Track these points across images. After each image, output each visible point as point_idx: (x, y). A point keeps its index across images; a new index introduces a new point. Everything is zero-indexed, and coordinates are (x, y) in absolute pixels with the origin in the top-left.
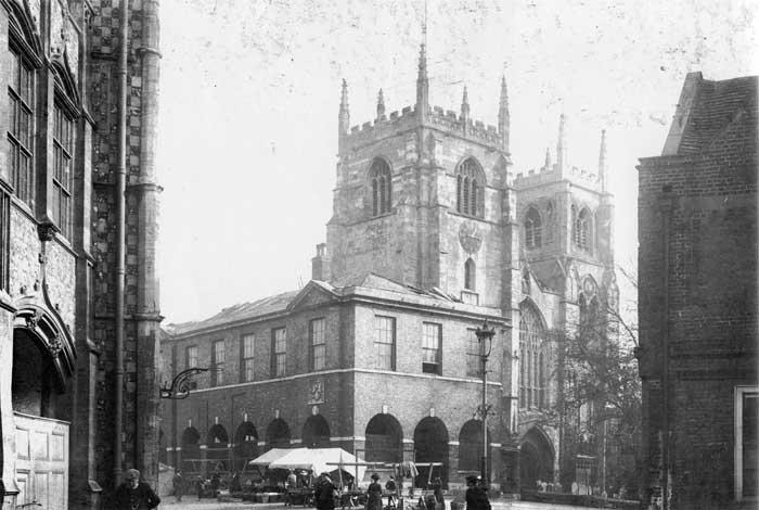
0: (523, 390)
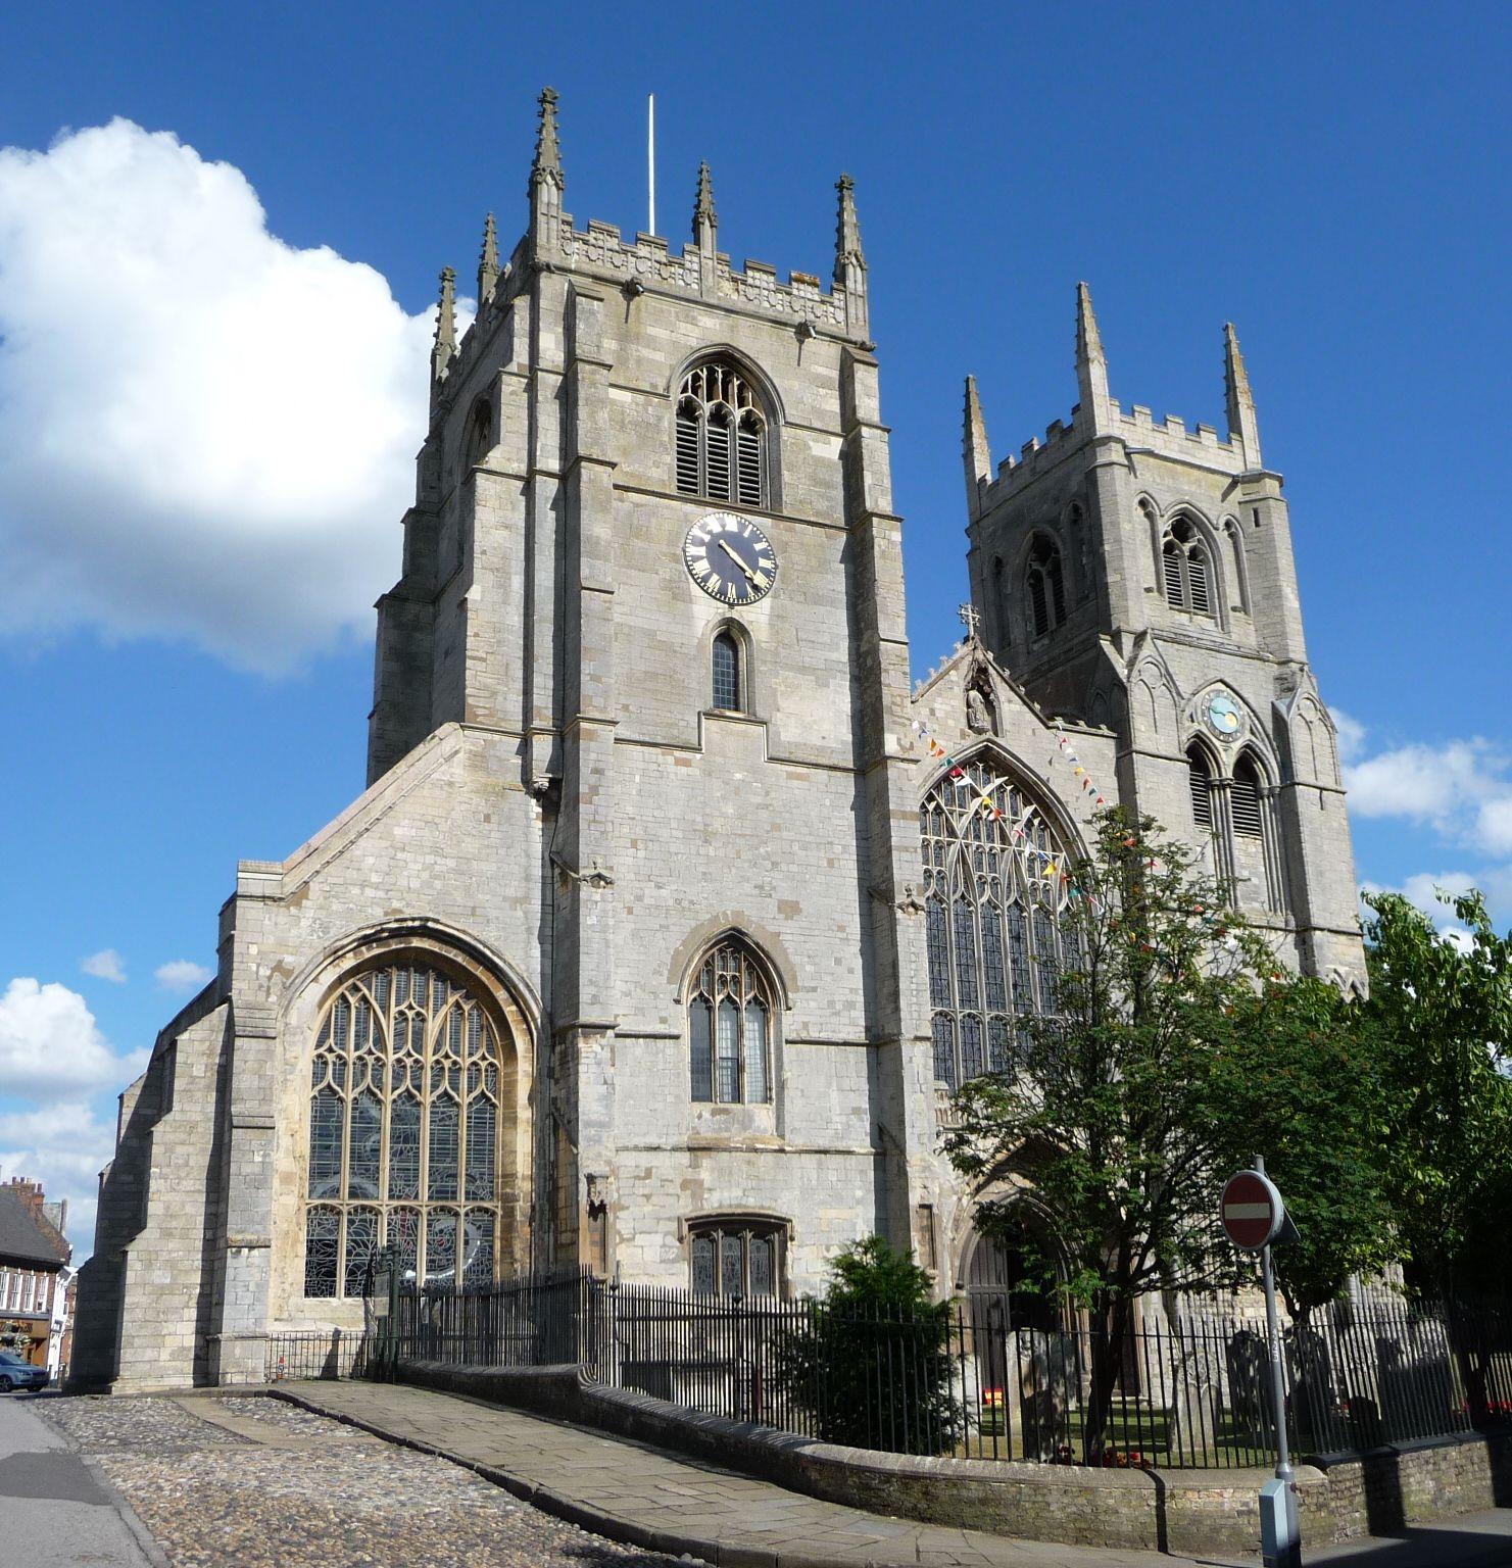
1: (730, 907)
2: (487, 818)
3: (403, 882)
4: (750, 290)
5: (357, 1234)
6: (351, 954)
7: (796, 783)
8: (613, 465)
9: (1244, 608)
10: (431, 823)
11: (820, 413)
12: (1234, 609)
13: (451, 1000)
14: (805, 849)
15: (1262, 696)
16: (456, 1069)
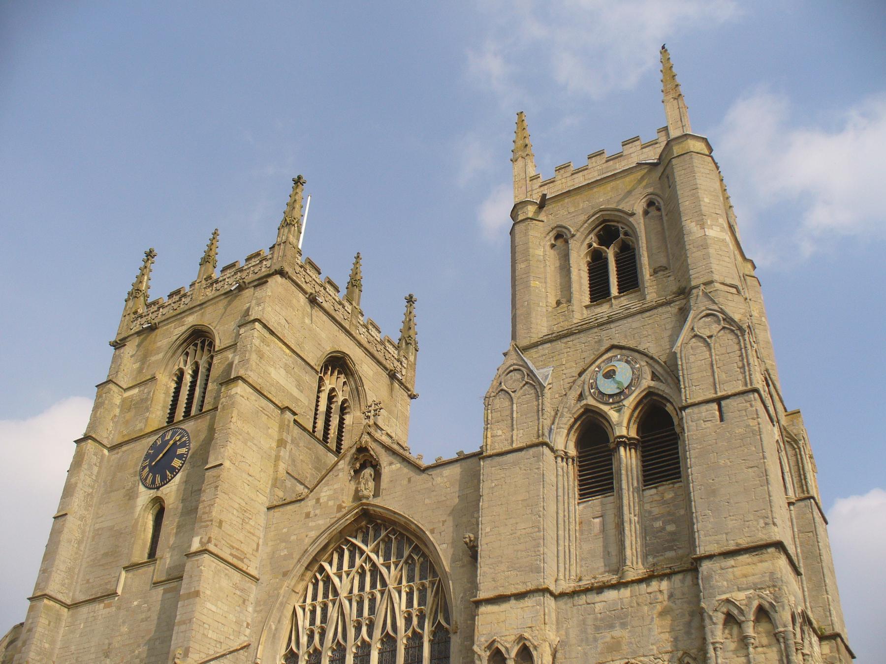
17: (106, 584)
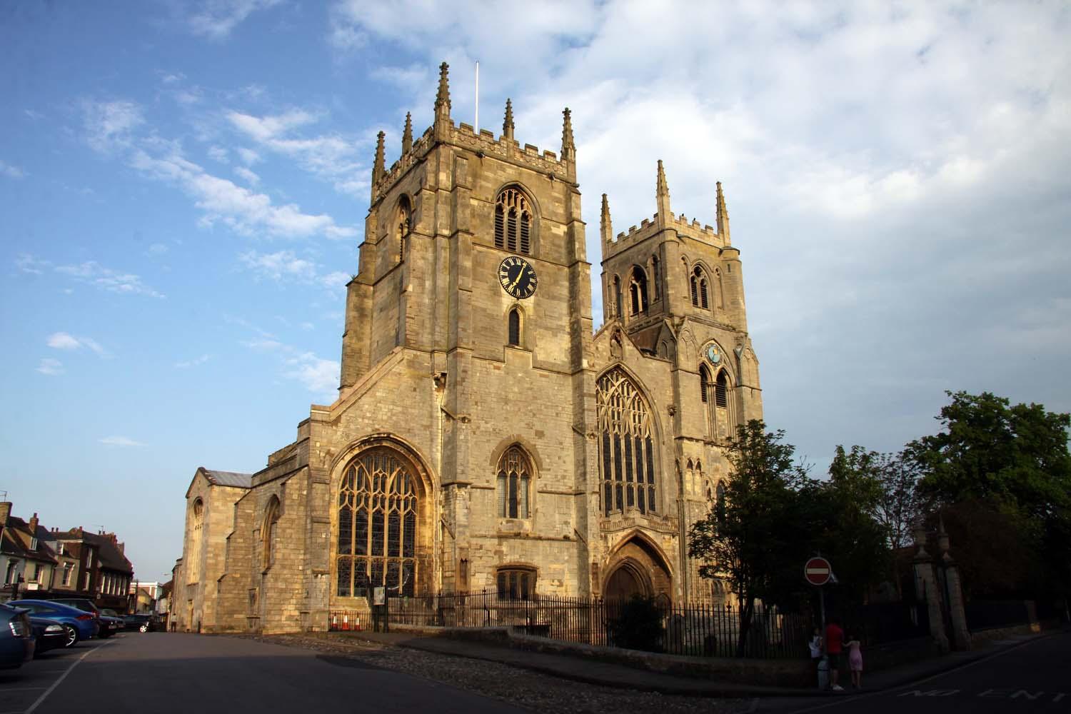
0: (608, 487)
1: (515, 433)
2: (415, 390)
3: (380, 417)
4: (527, 158)
5: (359, 570)
6: (357, 448)
7: (543, 379)
8: (472, 234)
9: (722, 308)
10: (391, 391)
11: (556, 214)
12: (719, 308)
13: (398, 470)
14: (546, 408)
15: (729, 345)
16: (399, 501)
17: (491, 351)
